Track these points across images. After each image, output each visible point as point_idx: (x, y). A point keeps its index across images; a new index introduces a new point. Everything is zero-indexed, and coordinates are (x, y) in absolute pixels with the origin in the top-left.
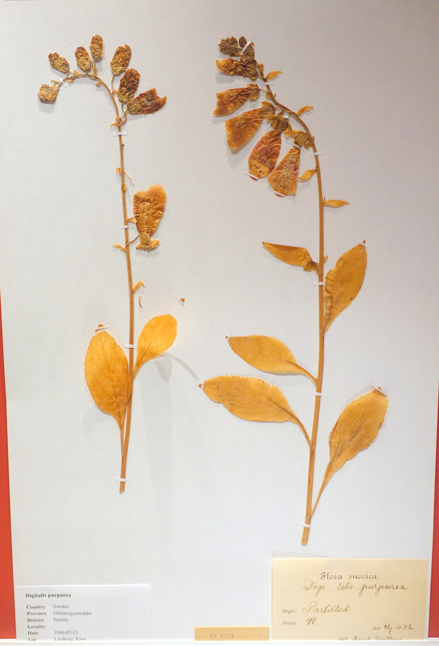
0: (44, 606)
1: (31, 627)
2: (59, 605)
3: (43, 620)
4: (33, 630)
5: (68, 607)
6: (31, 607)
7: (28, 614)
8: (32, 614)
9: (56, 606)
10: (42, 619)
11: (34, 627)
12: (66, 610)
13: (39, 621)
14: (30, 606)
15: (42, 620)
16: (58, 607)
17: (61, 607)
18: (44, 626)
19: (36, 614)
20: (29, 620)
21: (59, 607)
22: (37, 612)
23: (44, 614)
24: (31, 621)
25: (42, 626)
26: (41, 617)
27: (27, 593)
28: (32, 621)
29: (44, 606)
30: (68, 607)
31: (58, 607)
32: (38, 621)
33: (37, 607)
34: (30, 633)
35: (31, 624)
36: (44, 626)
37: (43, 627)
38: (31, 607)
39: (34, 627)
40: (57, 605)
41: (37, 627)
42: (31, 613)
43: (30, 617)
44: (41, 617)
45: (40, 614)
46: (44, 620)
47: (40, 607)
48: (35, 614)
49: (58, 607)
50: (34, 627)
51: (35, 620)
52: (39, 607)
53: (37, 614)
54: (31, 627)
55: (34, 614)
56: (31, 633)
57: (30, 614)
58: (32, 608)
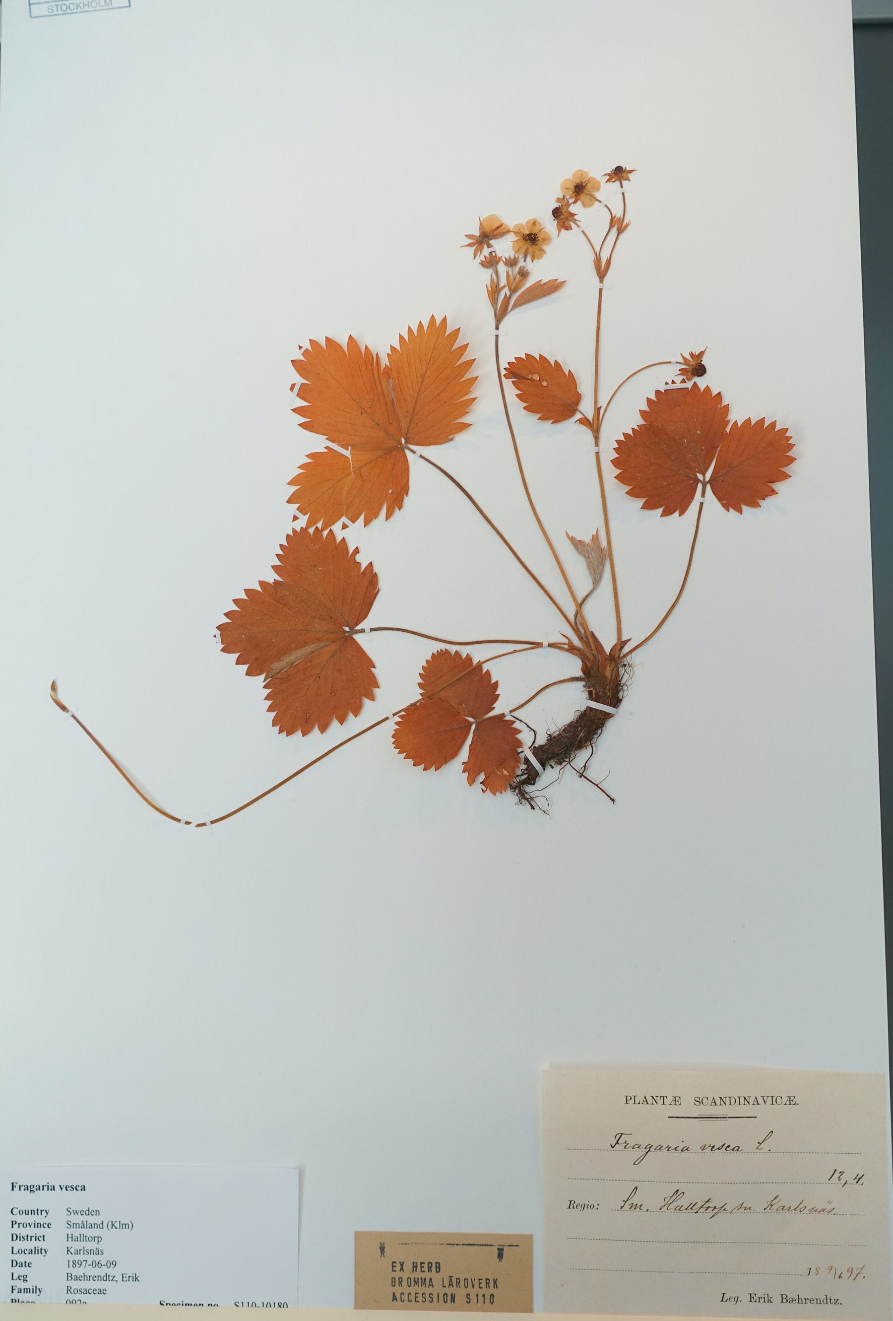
0: (46, 1211)
2: (79, 1209)
3: (44, 1236)
4: (21, 1258)
5: (97, 1212)
8: (21, 1225)
9: (73, 1211)
11: (24, 1251)
12: (92, 1219)
13: (36, 1240)
14: (17, 1208)
15: (42, 1237)
18: (45, 1250)
19: (30, 1226)
20: (15, 1237)
21: (79, 1213)
22: (31, 1221)
23: (47, 1228)
25: (41, 1249)
26: (40, 1232)
28: (22, 1239)
29: (46, 1211)
30: (97, 1212)
32: (33, 1239)
33: (33, 1212)
34: (15, 1264)
35: (19, 1245)
36: (45, 1250)
37: (43, 1251)
38: (20, 1212)
41: (31, 1252)
42: (20, 1222)
43: (16, 1230)
44: (40, 1232)
45: (39, 1225)
46: (45, 1238)
47: (39, 1212)
48: (28, 1226)
49: (77, 1214)
51: (28, 1238)
52: (36, 1212)
56: (18, 1265)
57: (17, 1224)
58: (23, 1212)
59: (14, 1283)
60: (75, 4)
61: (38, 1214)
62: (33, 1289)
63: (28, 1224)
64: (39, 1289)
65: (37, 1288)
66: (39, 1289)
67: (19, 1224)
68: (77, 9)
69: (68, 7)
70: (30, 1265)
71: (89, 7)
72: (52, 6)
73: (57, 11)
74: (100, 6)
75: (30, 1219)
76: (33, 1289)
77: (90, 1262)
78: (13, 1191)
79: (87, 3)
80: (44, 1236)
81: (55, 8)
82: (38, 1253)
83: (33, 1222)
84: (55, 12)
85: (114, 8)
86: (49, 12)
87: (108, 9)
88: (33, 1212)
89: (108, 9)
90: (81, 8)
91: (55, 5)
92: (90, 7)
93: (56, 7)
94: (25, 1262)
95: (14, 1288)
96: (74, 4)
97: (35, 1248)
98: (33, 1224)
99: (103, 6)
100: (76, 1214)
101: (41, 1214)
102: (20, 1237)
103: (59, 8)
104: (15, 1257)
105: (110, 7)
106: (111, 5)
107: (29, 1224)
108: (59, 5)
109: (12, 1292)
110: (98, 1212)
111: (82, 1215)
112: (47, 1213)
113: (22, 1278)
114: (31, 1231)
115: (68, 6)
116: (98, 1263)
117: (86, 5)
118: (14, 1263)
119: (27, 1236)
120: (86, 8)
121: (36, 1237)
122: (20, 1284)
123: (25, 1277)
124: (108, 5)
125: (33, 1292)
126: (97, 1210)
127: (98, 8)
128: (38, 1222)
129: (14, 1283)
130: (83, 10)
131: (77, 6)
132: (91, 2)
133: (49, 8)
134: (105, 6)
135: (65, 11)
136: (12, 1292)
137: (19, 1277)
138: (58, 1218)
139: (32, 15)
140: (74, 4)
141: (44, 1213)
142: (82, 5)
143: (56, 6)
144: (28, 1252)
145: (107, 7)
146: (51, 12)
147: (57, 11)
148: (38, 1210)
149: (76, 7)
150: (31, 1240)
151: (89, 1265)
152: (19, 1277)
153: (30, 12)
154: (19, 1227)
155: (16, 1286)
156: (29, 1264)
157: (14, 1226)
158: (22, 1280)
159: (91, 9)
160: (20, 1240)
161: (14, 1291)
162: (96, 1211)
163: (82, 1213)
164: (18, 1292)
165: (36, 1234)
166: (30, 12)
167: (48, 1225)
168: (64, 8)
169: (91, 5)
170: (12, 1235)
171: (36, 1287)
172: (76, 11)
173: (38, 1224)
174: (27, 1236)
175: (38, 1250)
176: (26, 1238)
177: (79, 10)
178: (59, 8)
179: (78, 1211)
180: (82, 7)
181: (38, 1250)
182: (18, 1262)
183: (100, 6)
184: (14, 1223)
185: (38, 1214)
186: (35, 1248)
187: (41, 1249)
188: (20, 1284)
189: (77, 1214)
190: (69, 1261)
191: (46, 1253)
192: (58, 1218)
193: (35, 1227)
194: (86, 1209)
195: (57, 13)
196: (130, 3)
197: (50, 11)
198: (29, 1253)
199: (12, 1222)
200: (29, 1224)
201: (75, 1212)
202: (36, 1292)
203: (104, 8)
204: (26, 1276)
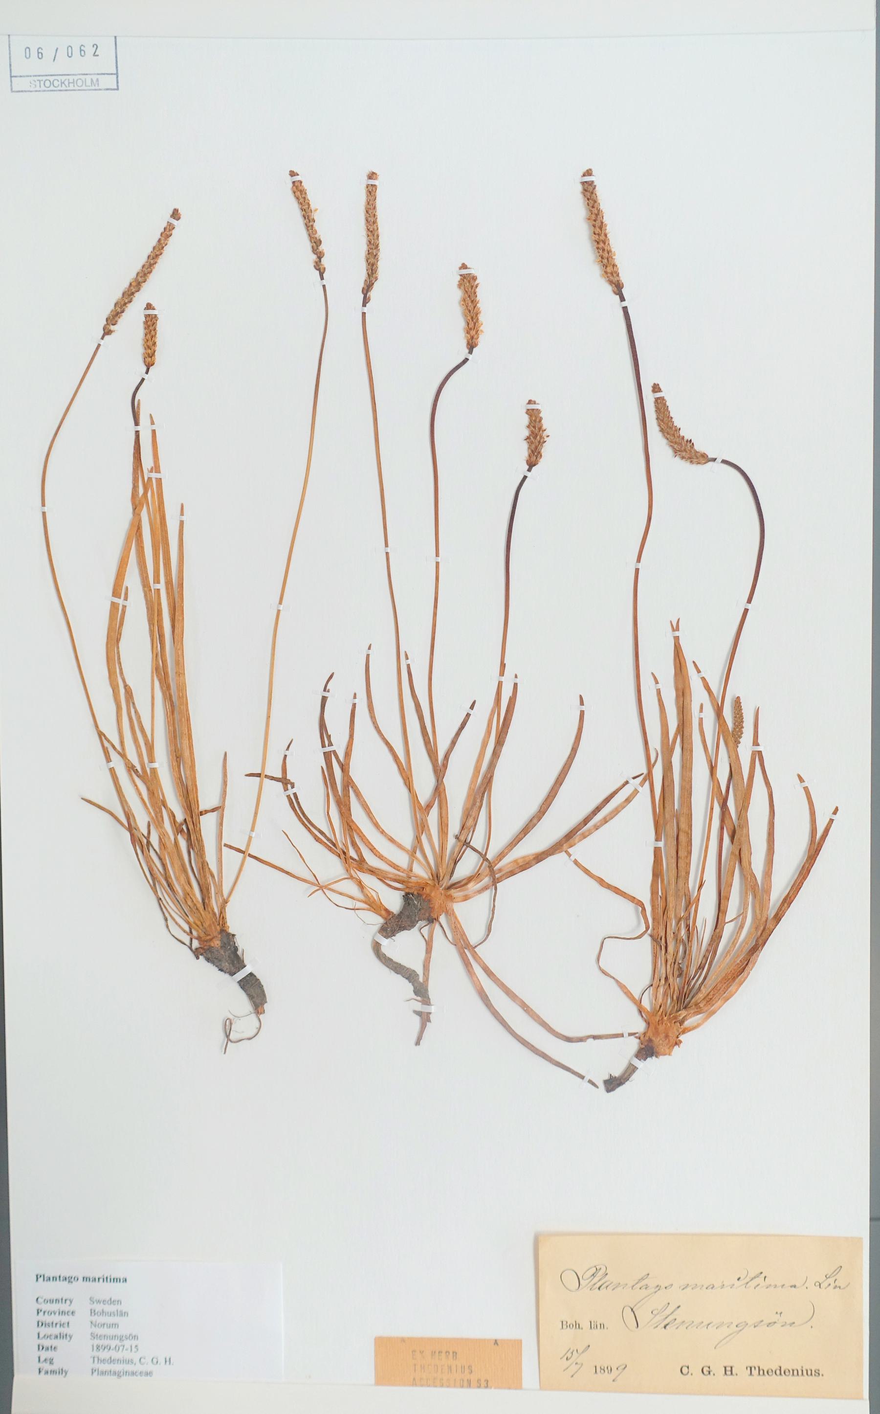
0: (70, 1300)
1: (45, 1336)
3: (68, 1323)
4: (47, 1343)
6: (46, 1301)
7: (38, 1313)
8: (46, 1313)
10: (67, 1322)
15: (67, 1324)
16: (99, 1302)
19: (55, 1314)
20: (40, 1324)
24: (44, 1325)
25: (66, 1335)
26: (64, 1319)
31: (99, 1302)
33: (57, 1301)
34: (41, 1348)
35: (44, 1331)
36: (69, 1336)
37: (68, 1336)
39: (49, 1337)
43: (41, 1317)
44: (64, 1319)
45: (63, 1313)
47: (64, 1301)
48: (53, 1314)
49: (100, 1303)
50: (49, 1337)
52: (60, 1301)
53: (57, 1313)
56: (44, 1349)
57: (42, 1312)
58: (47, 1302)
59: (40, 1365)
60: (60, 80)
65: (64, 1370)
67: (44, 1312)
69: (52, 83)
71: (74, 86)
72: (35, 81)
73: (40, 86)
74: (86, 86)
75: (55, 1307)
77: (113, 1347)
79: (72, 81)
83: (58, 1311)
84: (38, 88)
85: (100, 90)
87: (96, 90)
89: (96, 90)
90: (66, 87)
91: (38, 80)
93: (38, 82)
95: (41, 1370)
96: (58, 81)
99: (89, 86)
103: (42, 83)
105: (97, 87)
108: (42, 80)
115: (52, 82)
117: (72, 83)
120: (71, 87)
122: (47, 1366)
124: (95, 86)
127: (84, 87)
129: (40, 1365)
130: (68, 88)
131: (61, 83)
135: (48, 87)
138: (82, 1307)
140: (58, 81)
142: (66, 83)
145: (93, 88)
147: (40, 86)
149: (60, 84)
159: (76, 88)
168: (47, 84)
171: (62, 1370)
172: (60, 88)
177: (64, 88)
178: (42, 83)
180: (67, 85)
188: (47, 1366)
192: (82, 1307)
196: (118, 86)
203: (91, 88)
204: (52, 1360)
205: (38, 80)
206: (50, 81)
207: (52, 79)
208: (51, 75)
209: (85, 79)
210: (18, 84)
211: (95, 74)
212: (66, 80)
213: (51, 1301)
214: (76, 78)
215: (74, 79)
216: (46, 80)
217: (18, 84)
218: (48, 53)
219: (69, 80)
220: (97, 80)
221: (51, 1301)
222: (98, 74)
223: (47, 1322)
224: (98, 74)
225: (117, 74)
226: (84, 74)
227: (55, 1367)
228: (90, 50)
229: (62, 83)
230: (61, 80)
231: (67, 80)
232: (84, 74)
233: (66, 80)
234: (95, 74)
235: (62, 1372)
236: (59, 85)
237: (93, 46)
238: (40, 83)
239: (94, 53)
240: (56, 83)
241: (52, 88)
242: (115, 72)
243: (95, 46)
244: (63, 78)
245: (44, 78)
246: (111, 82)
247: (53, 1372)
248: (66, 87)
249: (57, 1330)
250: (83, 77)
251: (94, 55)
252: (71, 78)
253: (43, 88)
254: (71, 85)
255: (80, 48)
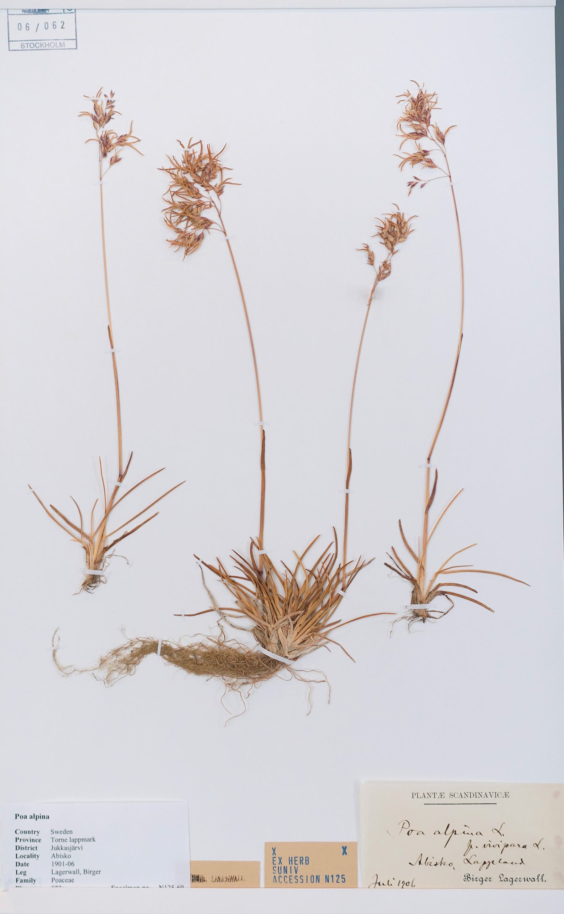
0: (38, 832)
1: (21, 856)
2: (59, 830)
3: (36, 847)
4: (22, 861)
5: (71, 832)
8: (22, 840)
9: (55, 831)
13: (31, 849)
15: (35, 848)
17: (61, 833)
18: (37, 856)
19: (28, 841)
21: (59, 833)
22: (28, 838)
23: (38, 842)
25: (35, 855)
26: (34, 844)
27: (16, 813)
28: (22, 849)
29: (38, 832)
30: (71, 832)
32: (30, 849)
33: (29, 832)
34: (18, 864)
35: (20, 853)
36: (37, 856)
37: (36, 856)
40: (56, 829)
42: (21, 838)
43: (19, 843)
44: (34, 844)
45: (33, 840)
47: (33, 832)
48: (26, 841)
49: (58, 833)
51: (26, 848)
52: (31, 832)
53: (29, 841)
54: (21, 856)
55: (24, 840)
56: (20, 865)
57: (19, 840)
59: (17, 876)
61: (32, 833)
62: (30, 880)
63: (26, 840)
64: (34, 880)
66: (34, 880)
67: (20, 840)
68: (41, 47)
70: (28, 865)
71: (49, 47)
73: (27, 47)
75: (28, 836)
76: (30, 880)
77: (66, 863)
78: (16, 819)
79: (48, 44)
80: (36, 847)
81: (26, 45)
82: (33, 857)
83: (30, 839)
84: (26, 48)
85: (65, 49)
86: (21, 47)
88: (29, 832)
90: (44, 47)
91: (26, 43)
92: (50, 46)
93: (26, 44)
94: (25, 863)
95: (18, 879)
96: (39, 44)
97: (31, 854)
98: (29, 840)
99: (58, 47)
100: (57, 833)
101: (35, 833)
102: (21, 848)
103: (29, 45)
104: (18, 860)
106: (64, 47)
107: (27, 839)
108: (29, 43)
109: (17, 882)
110: (71, 832)
111: (61, 834)
112: (38, 833)
113: (23, 873)
114: (28, 844)
116: (72, 863)
118: (18, 864)
119: (26, 847)
120: (47, 47)
121: (31, 848)
122: (22, 877)
123: (25, 872)
125: (30, 882)
126: (70, 830)
127: (55, 48)
128: (33, 838)
129: (17, 876)
130: (45, 48)
131: (41, 45)
132: (51, 43)
133: (22, 45)
134: (60, 47)
136: (17, 882)
137: (21, 873)
138: (45, 837)
139: (10, 49)
140: (39, 44)
141: (36, 833)
142: (44, 45)
143: (27, 44)
144: (27, 857)
145: (61, 48)
146: (23, 48)
147: (27, 47)
148: (32, 831)
149: (40, 46)
150: (28, 849)
151: (66, 865)
152: (21, 873)
153: (9, 47)
154: (20, 841)
155: (19, 878)
156: (27, 864)
157: (17, 841)
158: (23, 874)
159: (50, 48)
160: (21, 849)
161: (18, 881)
162: (70, 831)
163: (61, 833)
164: (21, 882)
165: (31, 846)
166: (9, 47)
167: (39, 840)
168: (32, 45)
169: (51, 45)
170: (16, 846)
171: (32, 879)
172: (40, 48)
173: (32, 840)
174: (26, 847)
175: (33, 856)
176: (25, 848)
177: (42, 48)
178: (29, 45)
179: (58, 832)
180: (45, 46)
181: (33, 856)
182: (20, 864)
183: (56, 47)
184: (17, 839)
185: (32, 833)
186: (31, 854)
187: (35, 855)
188: (22, 877)
189: (58, 833)
190: (53, 862)
191: (38, 857)
193: (30, 841)
194: (63, 830)
195: (27, 49)
196: (77, 47)
197: (23, 47)
198: (27, 858)
199: (16, 838)
200: (27, 839)
201: (56, 832)
202: (32, 882)
205: (26, 43)
206: (34, 44)
207: (35, 42)
208: (35, 40)
209: (56, 43)
210: (13, 46)
211: (62, 40)
212: (43, 43)
213: (25, 832)
214: (50, 42)
215: (49, 43)
216: (31, 43)
217: (13, 46)
218: (33, 27)
219: (45, 43)
220: (64, 42)
221: (25, 832)
222: (64, 40)
223: (22, 847)
224: (64, 40)
225: (76, 40)
226: (56, 40)
227: (27, 878)
228: (59, 25)
229: (41, 45)
230: (41, 43)
231: (44, 44)
232: (56, 40)
233: (43, 43)
234: (62, 40)
235: (32, 881)
236: (39, 46)
237: (61, 23)
238: (27, 45)
239: (62, 27)
240: (37, 45)
241: (35, 48)
242: (75, 38)
243: (63, 23)
244: (42, 42)
245: (30, 42)
246: (72, 44)
247: (26, 881)
248: (44, 47)
249: (28, 852)
250: (55, 42)
251: (62, 28)
252: (47, 42)
253: (29, 48)
254: (47, 46)
255: (53, 24)
